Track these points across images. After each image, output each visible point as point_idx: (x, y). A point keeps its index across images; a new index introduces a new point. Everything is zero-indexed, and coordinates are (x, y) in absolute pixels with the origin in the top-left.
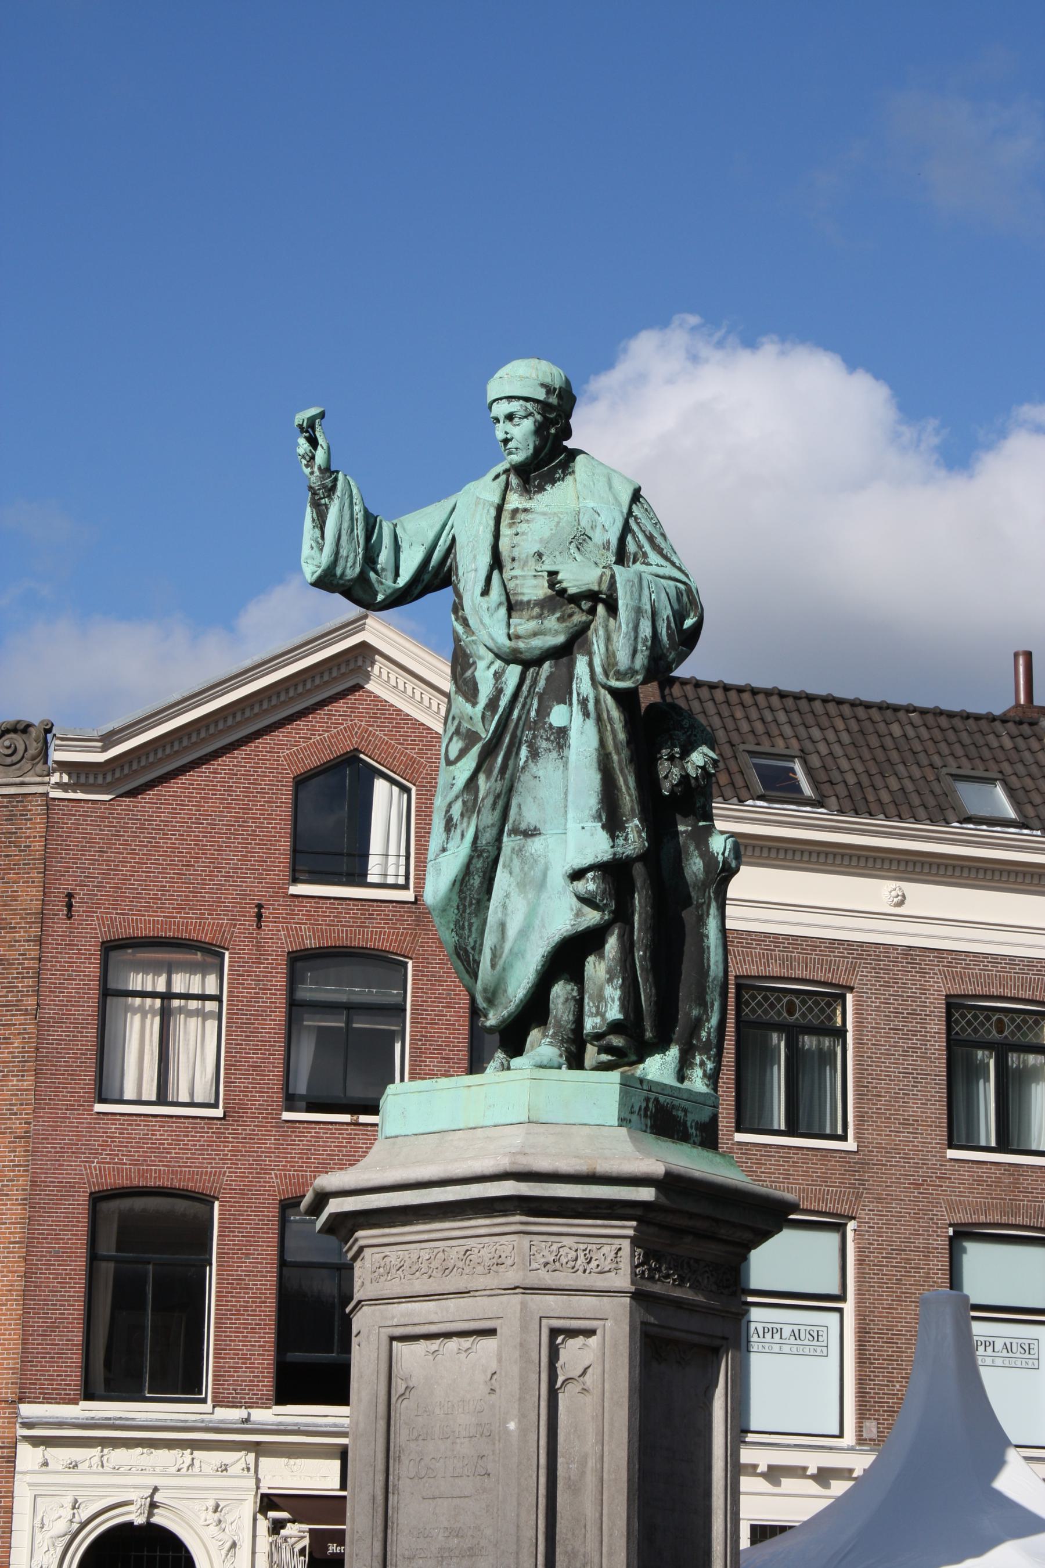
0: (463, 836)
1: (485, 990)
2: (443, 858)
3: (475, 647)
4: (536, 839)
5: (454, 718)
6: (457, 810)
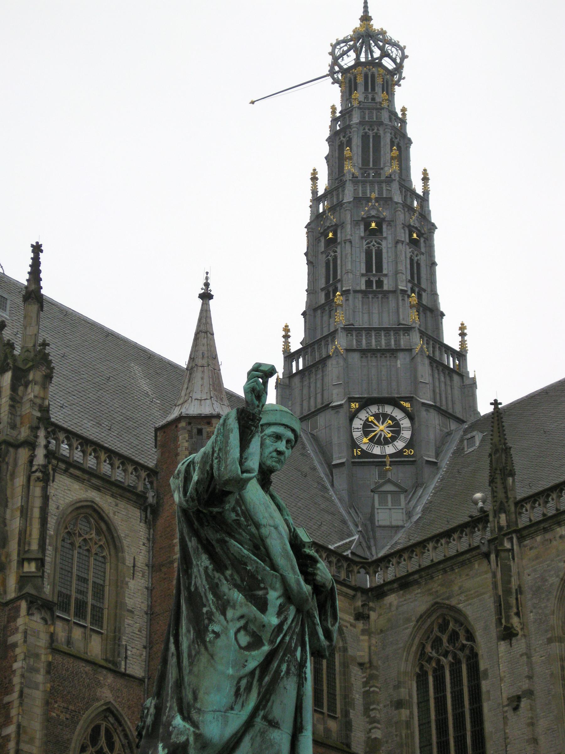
0: (243, 706)
2: (230, 714)
3: (274, 580)
4: (276, 731)
5: (242, 617)
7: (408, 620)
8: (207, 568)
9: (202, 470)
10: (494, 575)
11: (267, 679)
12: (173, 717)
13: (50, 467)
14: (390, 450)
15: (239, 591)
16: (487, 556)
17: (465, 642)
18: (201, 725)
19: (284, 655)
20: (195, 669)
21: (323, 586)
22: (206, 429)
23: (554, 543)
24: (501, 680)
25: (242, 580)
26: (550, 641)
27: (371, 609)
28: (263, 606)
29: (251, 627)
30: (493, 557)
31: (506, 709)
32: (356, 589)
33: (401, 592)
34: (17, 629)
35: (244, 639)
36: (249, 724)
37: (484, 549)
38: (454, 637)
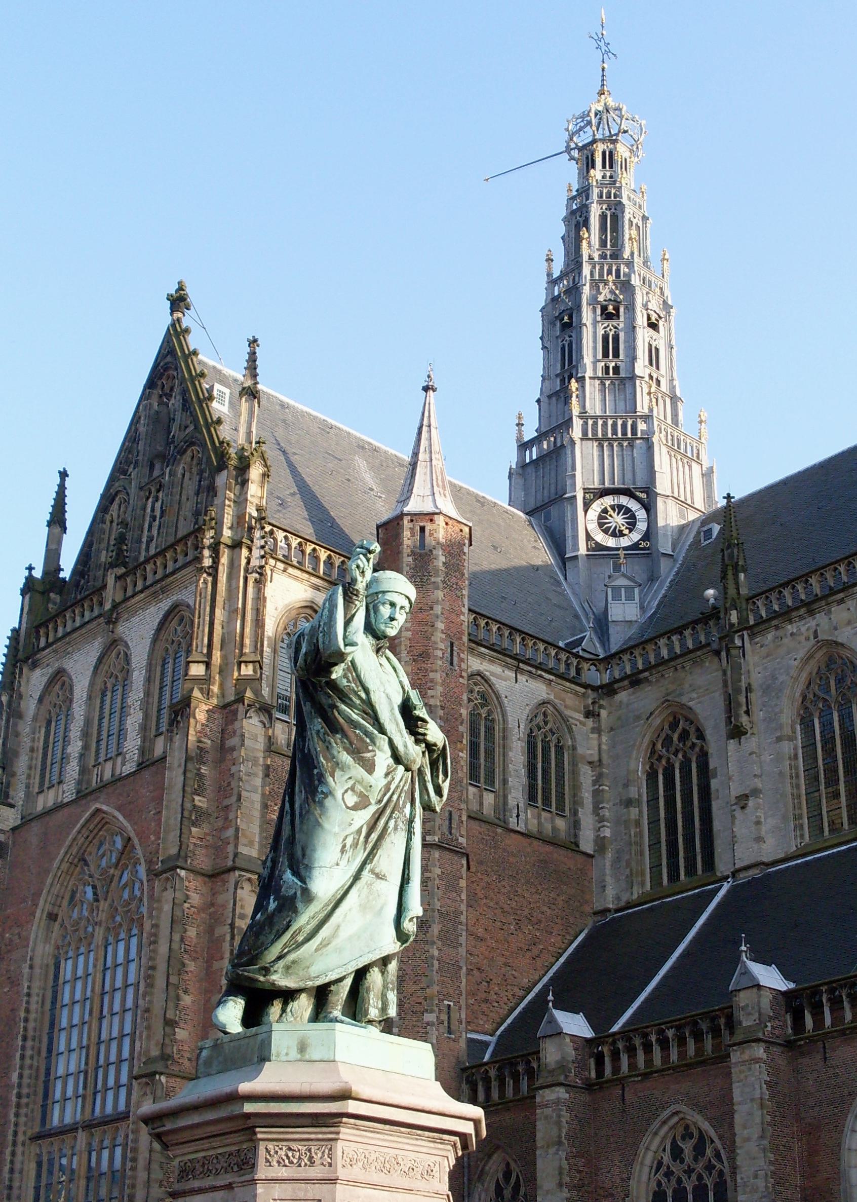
1: (294, 962)
3: (382, 742)
5: (350, 778)
6: (349, 841)
7: (638, 718)
8: (319, 731)
9: (309, 642)
10: (724, 673)
11: (374, 836)
12: (284, 872)
13: (268, 568)
14: (625, 542)
15: (348, 754)
16: (717, 653)
17: (695, 741)
18: (308, 880)
19: (392, 812)
20: (305, 827)
21: (435, 745)
22: (429, 527)
23: (785, 641)
24: (730, 778)
25: (351, 744)
26: (779, 739)
27: (601, 707)
28: (370, 767)
29: (359, 788)
30: (723, 654)
31: (734, 807)
32: (586, 686)
33: (632, 690)
34: (234, 732)
35: (351, 799)
36: (357, 877)
37: (715, 646)
38: (685, 735)
